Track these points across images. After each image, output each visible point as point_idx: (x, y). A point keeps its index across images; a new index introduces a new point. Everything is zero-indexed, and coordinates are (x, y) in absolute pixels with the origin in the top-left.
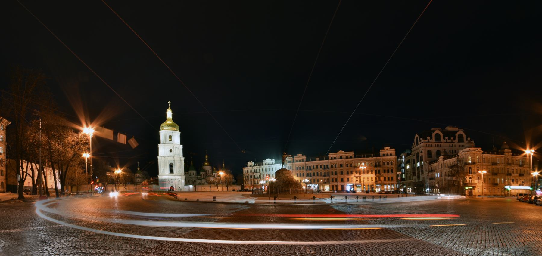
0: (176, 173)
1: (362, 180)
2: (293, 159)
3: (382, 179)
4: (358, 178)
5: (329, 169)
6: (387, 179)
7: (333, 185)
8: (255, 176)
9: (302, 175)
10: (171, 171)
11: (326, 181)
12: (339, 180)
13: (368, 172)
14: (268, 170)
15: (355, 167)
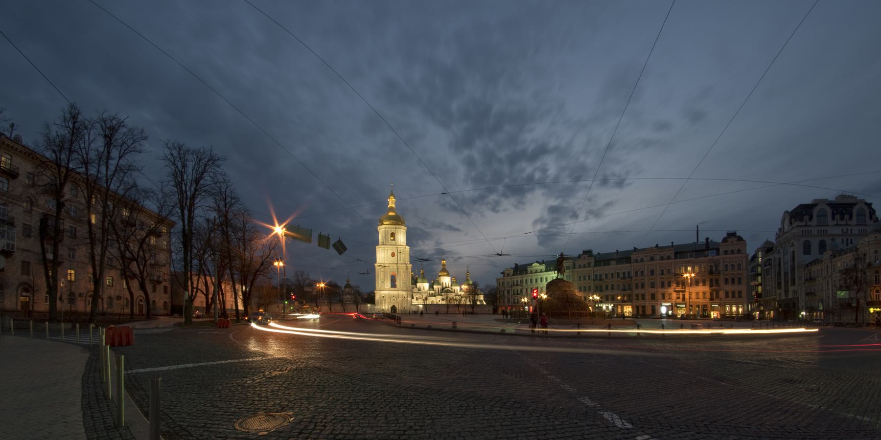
0: (400, 286)
1: (687, 296)
2: (574, 264)
3: (722, 294)
4: (681, 293)
5: (631, 278)
6: (730, 295)
7: (638, 305)
8: (514, 290)
9: (587, 289)
10: (393, 285)
11: (626, 299)
12: (648, 297)
13: (697, 284)
14: (534, 281)
15: (675, 275)
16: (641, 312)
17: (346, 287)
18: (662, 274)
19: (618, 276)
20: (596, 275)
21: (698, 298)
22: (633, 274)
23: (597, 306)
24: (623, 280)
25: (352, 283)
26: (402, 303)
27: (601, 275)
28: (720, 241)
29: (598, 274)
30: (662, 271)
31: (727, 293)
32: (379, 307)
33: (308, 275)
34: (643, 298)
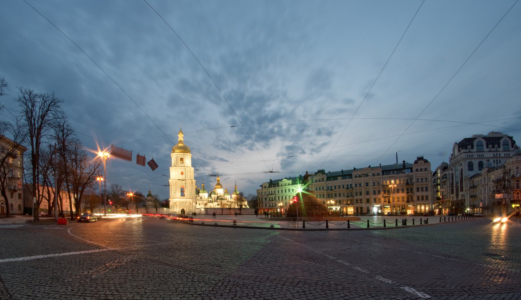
0: (188, 196)
1: (391, 200)
4: (387, 198)
5: (352, 188)
6: (420, 199)
8: (269, 198)
10: (183, 195)
11: (349, 203)
12: (364, 201)
13: (398, 191)
14: (284, 191)
16: (359, 211)
17: (148, 196)
18: (374, 185)
19: (343, 188)
20: (328, 187)
21: (398, 201)
22: (354, 186)
23: (329, 208)
24: (347, 190)
25: (153, 194)
26: (189, 207)
28: (413, 162)
29: (329, 186)
30: (374, 183)
31: (418, 197)
32: (172, 210)
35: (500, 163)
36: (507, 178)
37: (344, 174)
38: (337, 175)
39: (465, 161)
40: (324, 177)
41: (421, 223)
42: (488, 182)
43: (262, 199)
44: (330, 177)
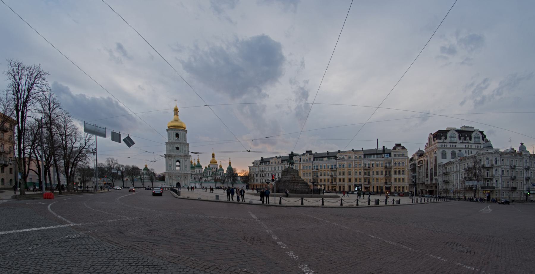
7: (340, 185)
8: (260, 174)
16: (342, 190)
17: (144, 169)
20: (314, 166)
22: (337, 166)
27: (317, 166)
28: (392, 149)
29: (316, 165)
33: (116, 161)
34: (344, 181)
35: (471, 153)
36: (477, 166)
37: (330, 155)
38: (323, 156)
39: (439, 150)
40: (310, 157)
41: (393, 203)
42: (460, 169)
43: (253, 175)
44: (317, 158)
